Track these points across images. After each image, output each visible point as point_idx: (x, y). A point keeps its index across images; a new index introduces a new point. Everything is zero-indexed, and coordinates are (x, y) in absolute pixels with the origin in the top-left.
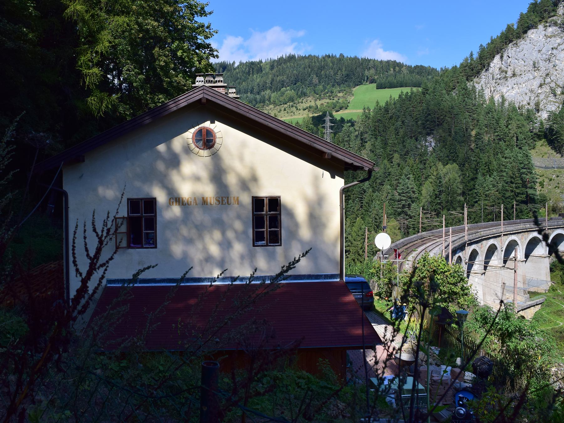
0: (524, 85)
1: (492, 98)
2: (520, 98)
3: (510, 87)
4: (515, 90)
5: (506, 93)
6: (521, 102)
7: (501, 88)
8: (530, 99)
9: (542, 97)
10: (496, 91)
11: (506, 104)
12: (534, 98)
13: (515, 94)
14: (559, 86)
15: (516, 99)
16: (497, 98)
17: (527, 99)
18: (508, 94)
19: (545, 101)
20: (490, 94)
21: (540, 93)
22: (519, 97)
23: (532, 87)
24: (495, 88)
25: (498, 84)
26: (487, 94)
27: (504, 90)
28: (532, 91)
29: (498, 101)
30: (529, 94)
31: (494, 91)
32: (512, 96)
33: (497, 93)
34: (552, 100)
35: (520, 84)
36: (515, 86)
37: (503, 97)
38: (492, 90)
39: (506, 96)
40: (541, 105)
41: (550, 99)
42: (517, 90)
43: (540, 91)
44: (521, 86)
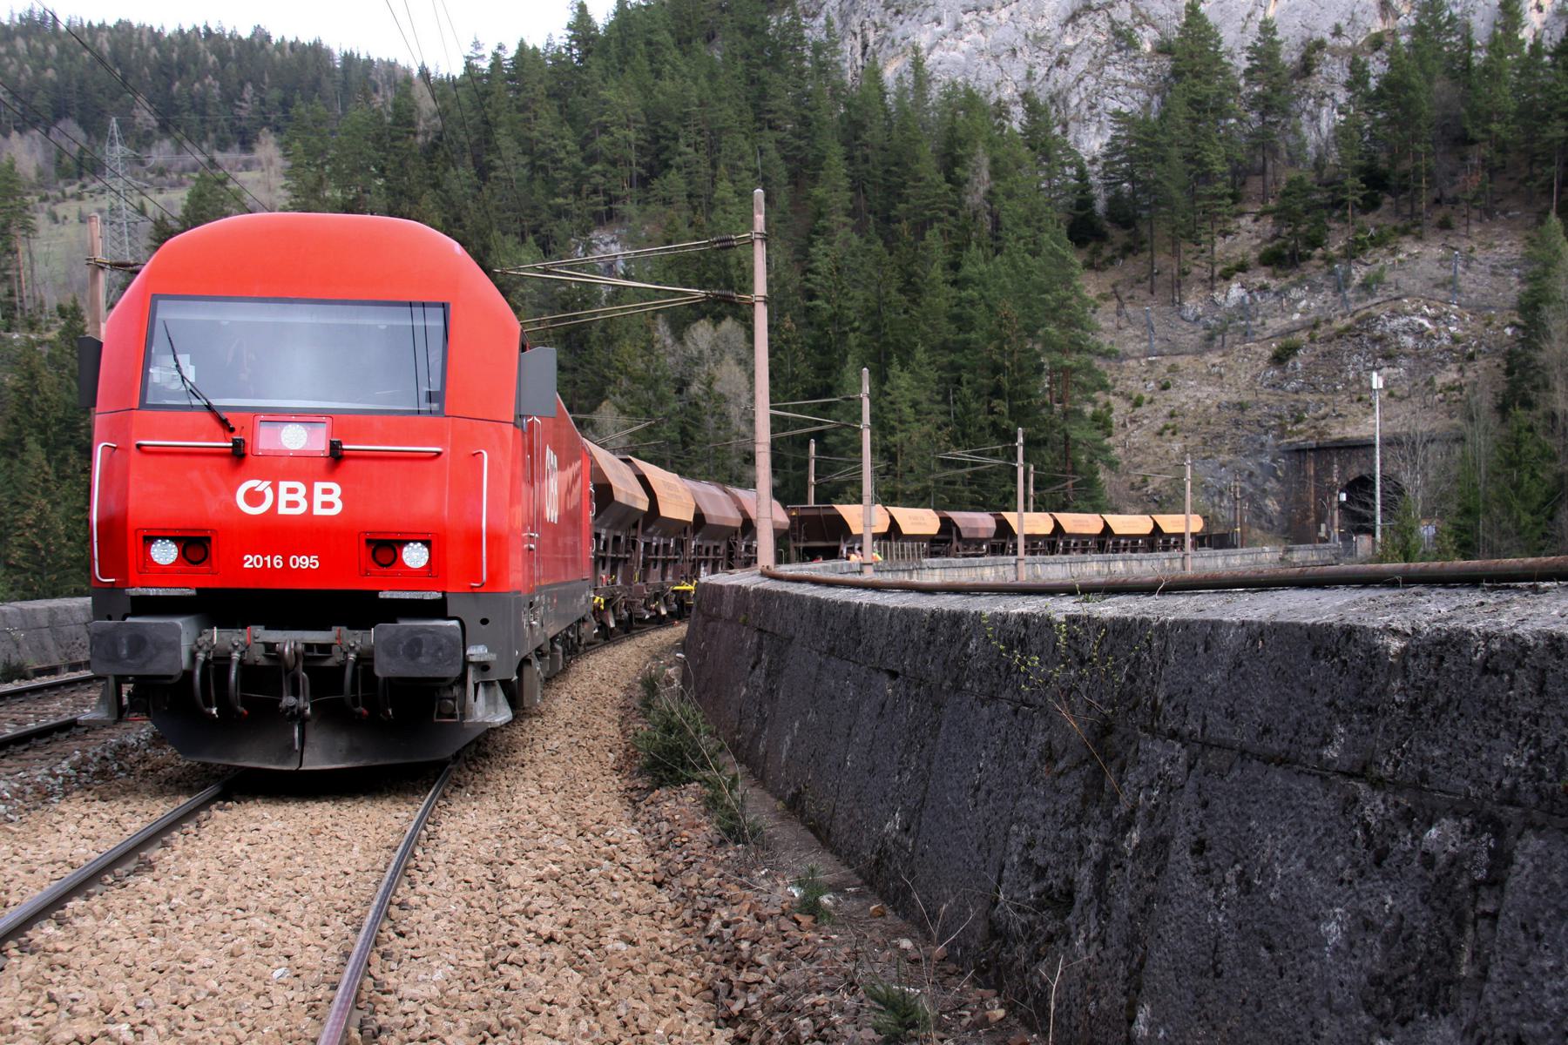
0: (1004, 14)
1: (874, 74)
2: (989, 73)
3: (946, 26)
4: (967, 38)
5: (931, 49)
6: (993, 88)
7: (911, 30)
8: (1030, 76)
9: (1079, 64)
10: (888, 43)
11: (934, 93)
12: (1044, 71)
13: (969, 57)
14: (1145, 20)
15: (972, 78)
16: (893, 70)
17: (1017, 72)
18: (937, 54)
19: (1090, 81)
20: (860, 62)
21: (1071, 51)
22: (985, 67)
23: (1039, 25)
24: (882, 32)
25: (898, 13)
26: (849, 57)
27: (924, 40)
28: (1038, 41)
29: (900, 79)
30: (1025, 56)
31: (883, 39)
32: (956, 63)
33: (891, 52)
34: (1119, 75)
35: (990, 9)
36: (966, 18)
37: (917, 64)
38: (871, 44)
39: (931, 60)
40: (1074, 101)
41: (1110, 70)
42: (976, 35)
43: (1069, 42)
44: (993, 18)
